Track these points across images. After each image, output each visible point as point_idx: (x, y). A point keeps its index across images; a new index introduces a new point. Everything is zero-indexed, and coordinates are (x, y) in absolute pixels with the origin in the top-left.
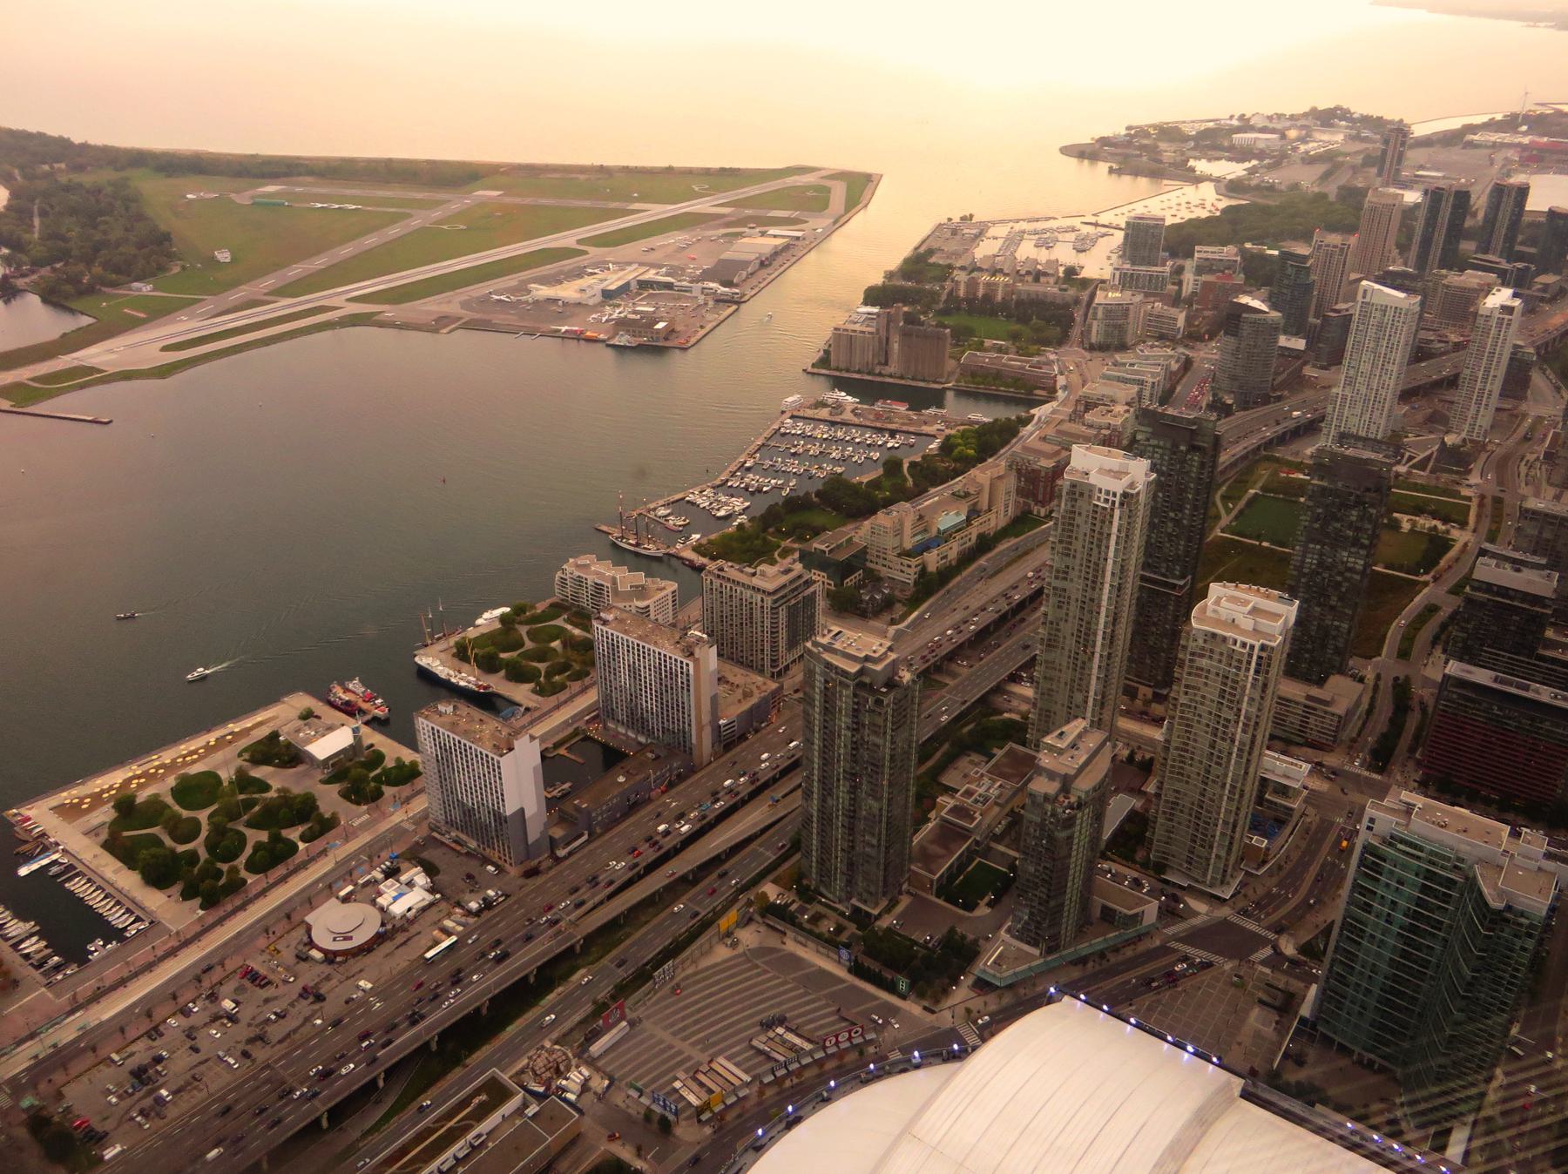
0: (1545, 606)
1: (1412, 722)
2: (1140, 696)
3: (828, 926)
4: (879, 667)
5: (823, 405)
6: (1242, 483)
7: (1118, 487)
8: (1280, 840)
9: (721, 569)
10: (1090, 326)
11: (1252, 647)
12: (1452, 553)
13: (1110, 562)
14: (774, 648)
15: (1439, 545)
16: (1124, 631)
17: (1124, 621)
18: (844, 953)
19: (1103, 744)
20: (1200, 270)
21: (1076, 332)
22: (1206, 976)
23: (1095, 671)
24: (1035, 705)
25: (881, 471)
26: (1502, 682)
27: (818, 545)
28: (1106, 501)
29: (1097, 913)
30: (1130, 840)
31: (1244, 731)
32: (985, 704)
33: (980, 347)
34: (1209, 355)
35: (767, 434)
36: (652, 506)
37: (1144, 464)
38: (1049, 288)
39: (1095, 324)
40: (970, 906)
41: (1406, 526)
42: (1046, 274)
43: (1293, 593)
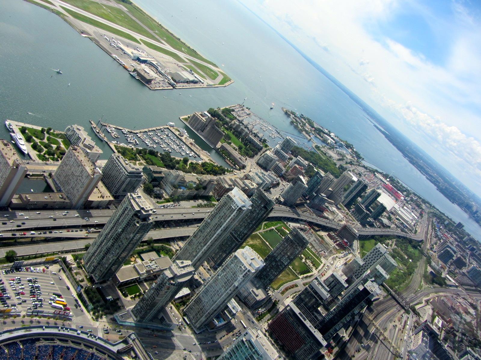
3: (79, 278)
4: (144, 213)
5: (179, 131)
7: (240, 204)
9: (119, 157)
11: (246, 269)
12: (309, 274)
13: (225, 223)
14: (119, 189)
15: (308, 270)
17: (219, 241)
18: (80, 287)
24: (181, 249)
25: (182, 159)
26: (301, 315)
27: (152, 168)
28: (235, 207)
29: (160, 317)
31: (230, 290)
32: (168, 240)
33: (230, 144)
34: (286, 186)
35: (158, 128)
36: (111, 126)
40: (126, 296)
41: (304, 260)
42: (258, 137)
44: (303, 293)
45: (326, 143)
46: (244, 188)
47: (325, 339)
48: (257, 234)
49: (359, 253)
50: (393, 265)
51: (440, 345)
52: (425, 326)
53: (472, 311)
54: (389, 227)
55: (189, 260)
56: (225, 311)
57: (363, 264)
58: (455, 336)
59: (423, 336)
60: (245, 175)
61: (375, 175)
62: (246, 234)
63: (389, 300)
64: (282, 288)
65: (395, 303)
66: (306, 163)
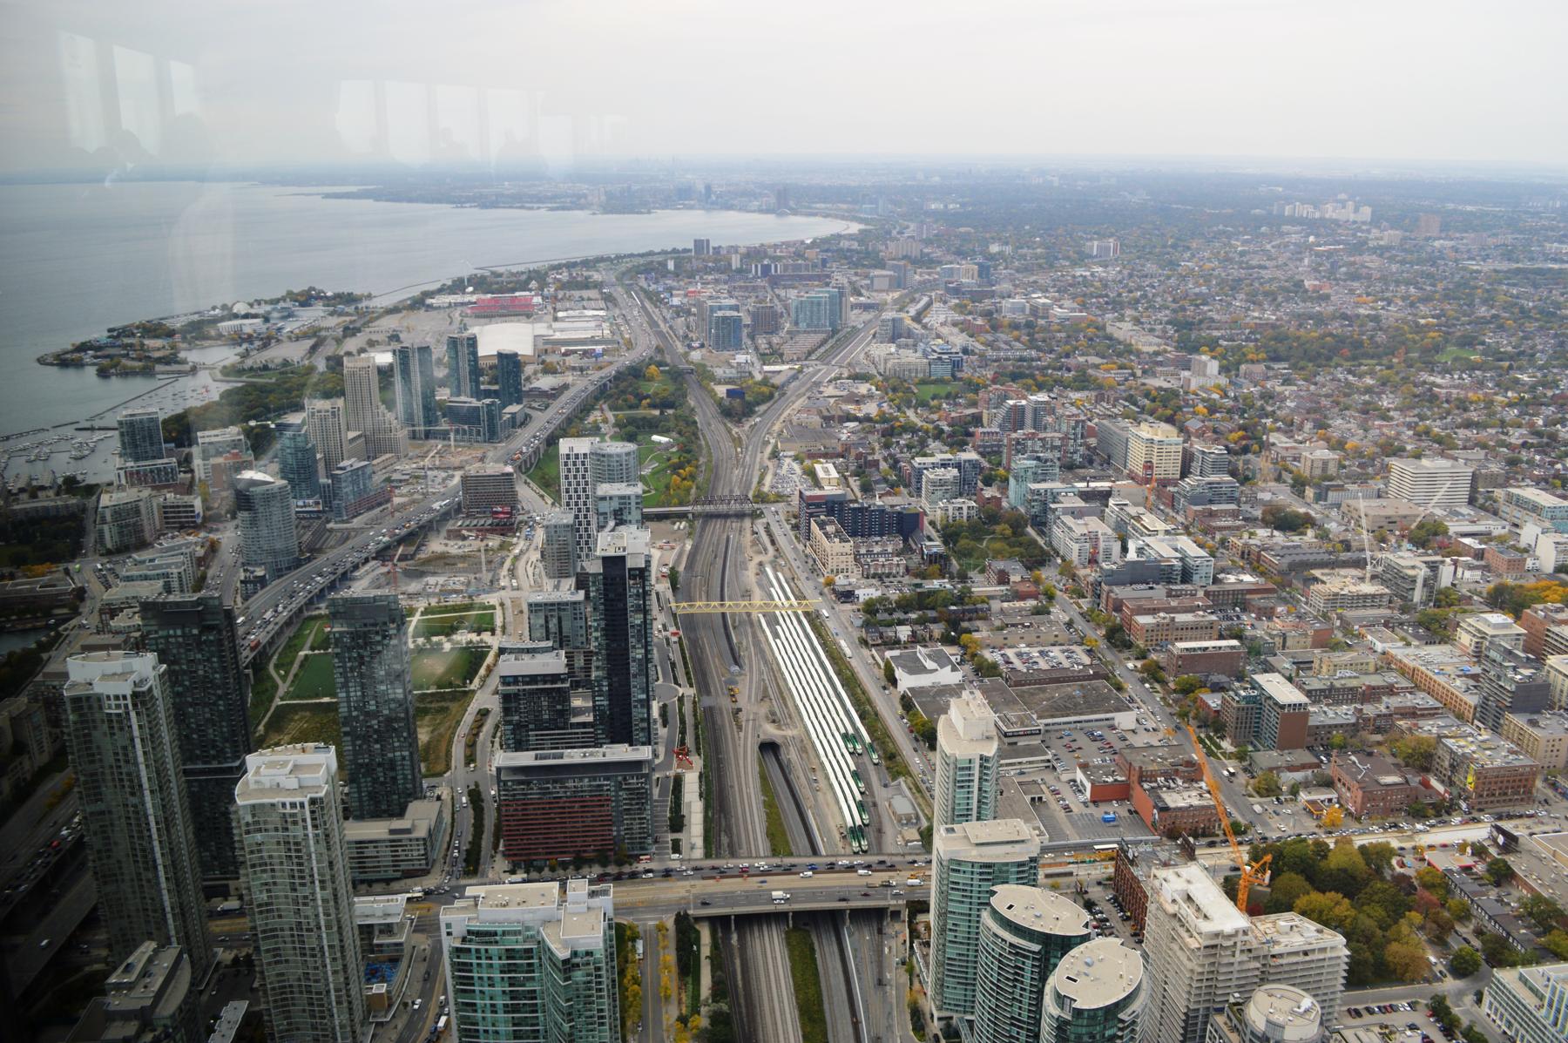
0: (563, 681)
6: (292, 647)
7: (126, 689)
8: (398, 977)
10: (101, 532)
12: (489, 660)
13: (142, 767)
16: (183, 831)
21: (90, 540)
23: (164, 885)
28: (118, 707)
31: (323, 888)
37: (150, 658)
38: (47, 501)
39: (106, 527)
41: (447, 646)
42: (42, 488)
46: (125, 642)
47: (643, 744)
50: (628, 454)
51: (861, 510)
52: (808, 505)
53: (863, 388)
54: (566, 387)
55: (143, 942)
57: (577, 517)
58: (876, 464)
59: (822, 525)
60: (101, 612)
61: (430, 307)
64: (458, 751)
65: (719, 523)
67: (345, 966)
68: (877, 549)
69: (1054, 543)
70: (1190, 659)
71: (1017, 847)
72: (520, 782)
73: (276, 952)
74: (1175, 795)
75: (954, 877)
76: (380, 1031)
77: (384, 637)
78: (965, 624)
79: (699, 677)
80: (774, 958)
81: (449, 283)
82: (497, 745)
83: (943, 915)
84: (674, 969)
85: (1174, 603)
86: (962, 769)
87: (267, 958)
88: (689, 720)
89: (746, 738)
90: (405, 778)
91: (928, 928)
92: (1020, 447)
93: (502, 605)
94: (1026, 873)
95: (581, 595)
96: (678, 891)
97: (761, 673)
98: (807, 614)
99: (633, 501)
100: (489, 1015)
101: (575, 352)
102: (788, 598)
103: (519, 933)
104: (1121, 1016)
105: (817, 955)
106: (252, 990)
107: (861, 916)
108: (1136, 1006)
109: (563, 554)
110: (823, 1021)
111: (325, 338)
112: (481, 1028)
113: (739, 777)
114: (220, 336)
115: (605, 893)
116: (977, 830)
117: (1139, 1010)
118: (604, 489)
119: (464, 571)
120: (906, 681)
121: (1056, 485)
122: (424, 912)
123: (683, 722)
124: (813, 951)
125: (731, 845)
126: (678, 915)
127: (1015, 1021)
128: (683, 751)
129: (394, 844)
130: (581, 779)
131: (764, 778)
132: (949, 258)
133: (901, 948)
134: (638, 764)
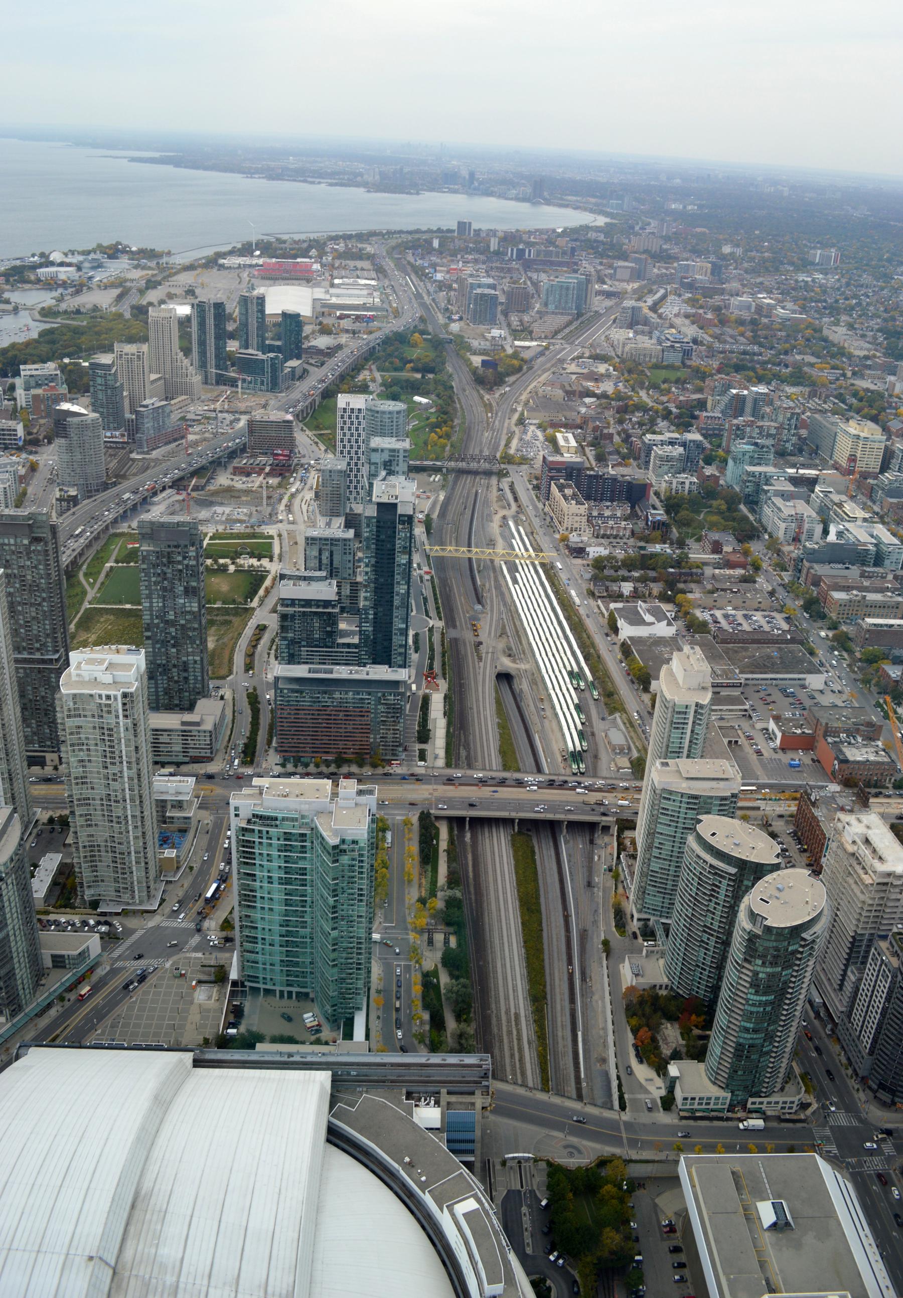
0: (334, 607)
1: (265, 720)
2: (48, 762)
6: (99, 559)
8: (186, 845)
12: (268, 582)
15: (256, 579)
19: (10, 818)
20: (27, 389)
22: (151, 980)
29: (48, 963)
30: (65, 889)
31: (129, 768)
34: (49, 457)
41: (232, 568)
43: (138, 644)
44: (283, 628)
45: (59, 286)
47: (400, 666)
48: (86, 609)
49: (326, 451)
50: (398, 412)
51: (596, 477)
52: (550, 469)
53: (602, 368)
54: (339, 347)
56: (168, 814)
57: (349, 464)
58: (610, 437)
59: (561, 488)
61: (222, 266)
62: (54, 631)
63: (455, 483)
64: (239, 659)
65: (469, 478)
66: (51, 367)
67: (144, 833)
68: (607, 513)
69: (764, 520)
70: (878, 633)
71: (722, 783)
72: (296, 691)
73: (87, 817)
74: (854, 751)
75: (665, 804)
76: (170, 887)
77: (185, 558)
78: (681, 586)
79: (448, 612)
80: (501, 856)
81: (239, 246)
82: (272, 656)
83: (651, 834)
84: (417, 859)
85: (866, 583)
86: (679, 713)
87: (80, 821)
88: (438, 648)
89: (485, 668)
90: (196, 679)
91: (633, 842)
92: (739, 434)
93: (280, 536)
94: (728, 806)
95: (351, 533)
96: (421, 793)
97: (500, 613)
98: (543, 565)
99: (401, 454)
100: (266, 885)
101: (348, 316)
102: (527, 550)
103: (296, 820)
104: (804, 935)
105: (537, 857)
106: (65, 845)
107: (576, 827)
108: (818, 928)
109: (334, 497)
110: (539, 911)
111: (130, 289)
112: (258, 895)
113: (477, 700)
114: (38, 281)
115: (371, 792)
116: (686, 765)
117: (820, 932)
118: (377, 442)
119: (247, 503)
120: (627, 631)
121: (770, 469)
122: (208, 793)
123: (432, 649)
124: (533, 853)
125: (468, 757)
126: (422, 813)
127: (706, 929)
128: (431, 674)
129: (185, 734)
130: (346, 693)
131: (499, 703)
132: (685, 255)
133: (609, 857)
134: (396, 684)
